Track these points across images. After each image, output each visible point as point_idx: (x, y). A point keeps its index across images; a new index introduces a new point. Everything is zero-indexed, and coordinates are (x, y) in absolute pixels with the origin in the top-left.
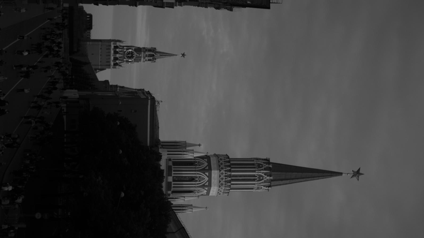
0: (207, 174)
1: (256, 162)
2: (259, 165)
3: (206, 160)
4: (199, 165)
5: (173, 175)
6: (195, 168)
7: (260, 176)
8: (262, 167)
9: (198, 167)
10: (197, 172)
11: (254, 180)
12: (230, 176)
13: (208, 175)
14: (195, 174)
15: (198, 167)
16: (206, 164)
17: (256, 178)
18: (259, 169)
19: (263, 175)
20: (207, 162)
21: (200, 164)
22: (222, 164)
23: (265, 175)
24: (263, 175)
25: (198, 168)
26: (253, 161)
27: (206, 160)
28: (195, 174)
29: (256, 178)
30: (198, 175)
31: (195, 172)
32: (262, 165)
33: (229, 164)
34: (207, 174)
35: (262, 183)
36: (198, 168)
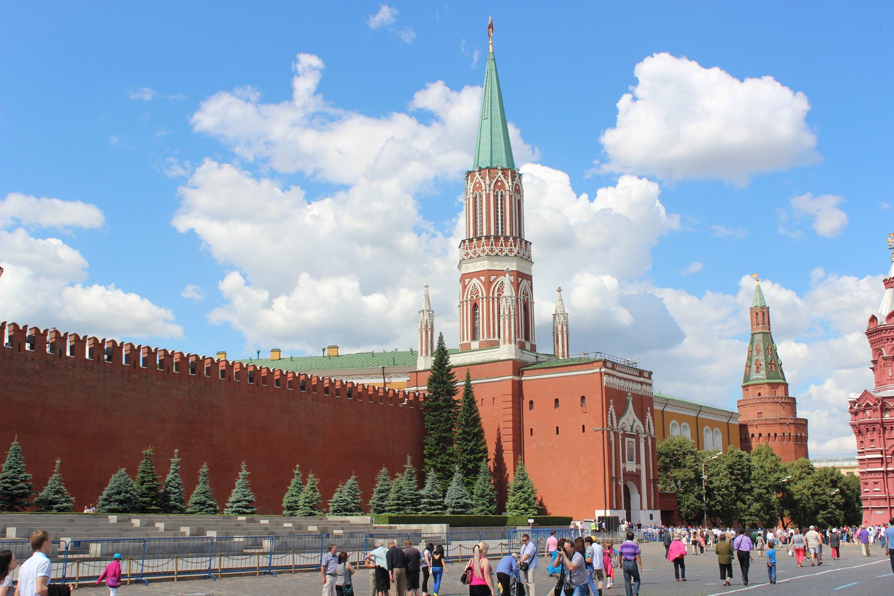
0: (520, 279)
1: (492, 192)
3: (492, 278)
5: (523, 340)
8: (501, 181)
9: (480, 295)
11: (519, 201)
15: (480, 295)
18: (507, 188)
20: (498, 276)
21: (475, 291)
22: (501, 251)
26: (489, 194)
27: (492, 278)
32: (497, 181)
34: (520, 279)
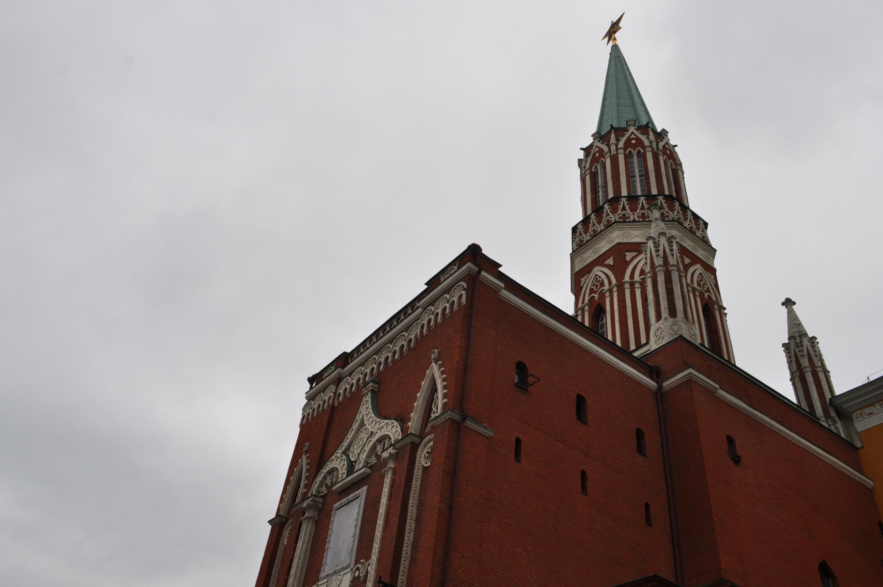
0: (629, 256)
2: (595, 160)
4: (602, 284)
6: (611, 291)
7: (628, 143)
10: (627, 278)
12: (632, 199)
13: (634, 254)
14: (632, 284)
16: (597, 270)
17: (635, 153)
19: (623, 140)
23: (623, 136)
24: (623, 140)
25: (610, 282)
28: (632, 284)
29: (635, 153)
30: (637, 278)
31: (627, 286)
33: (593, 216)
34: (629, 256)
35: (648, 138)
36: (610, 282)
